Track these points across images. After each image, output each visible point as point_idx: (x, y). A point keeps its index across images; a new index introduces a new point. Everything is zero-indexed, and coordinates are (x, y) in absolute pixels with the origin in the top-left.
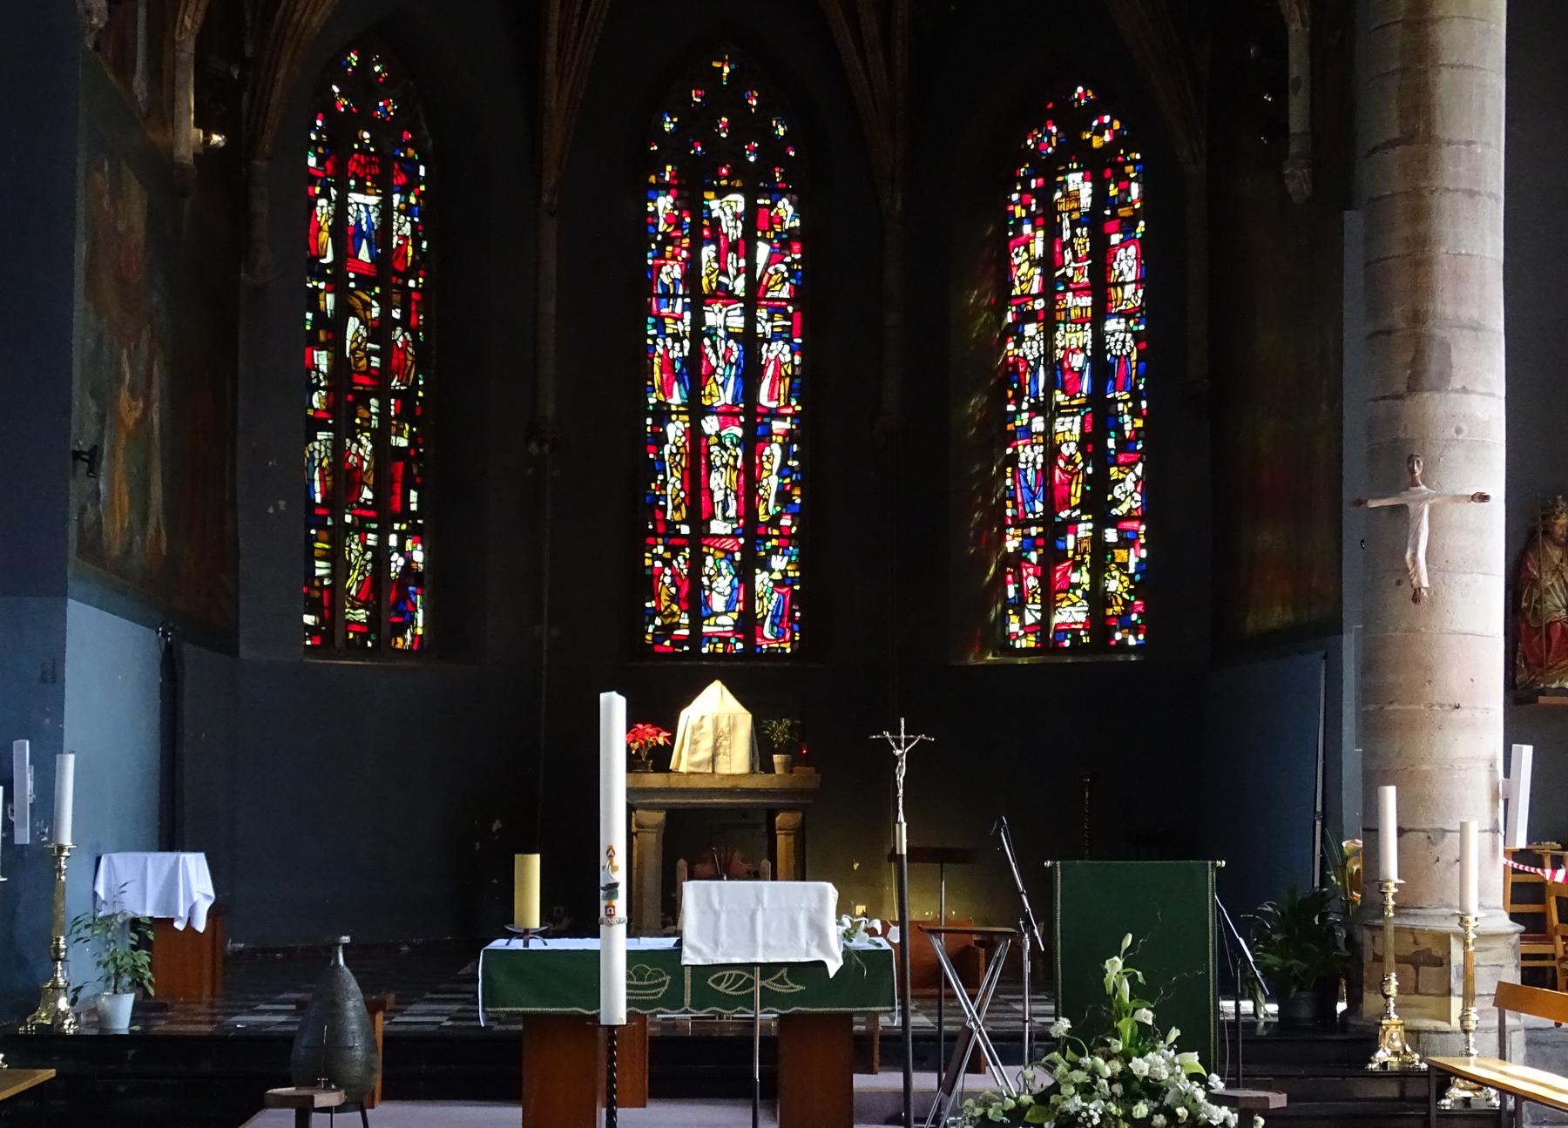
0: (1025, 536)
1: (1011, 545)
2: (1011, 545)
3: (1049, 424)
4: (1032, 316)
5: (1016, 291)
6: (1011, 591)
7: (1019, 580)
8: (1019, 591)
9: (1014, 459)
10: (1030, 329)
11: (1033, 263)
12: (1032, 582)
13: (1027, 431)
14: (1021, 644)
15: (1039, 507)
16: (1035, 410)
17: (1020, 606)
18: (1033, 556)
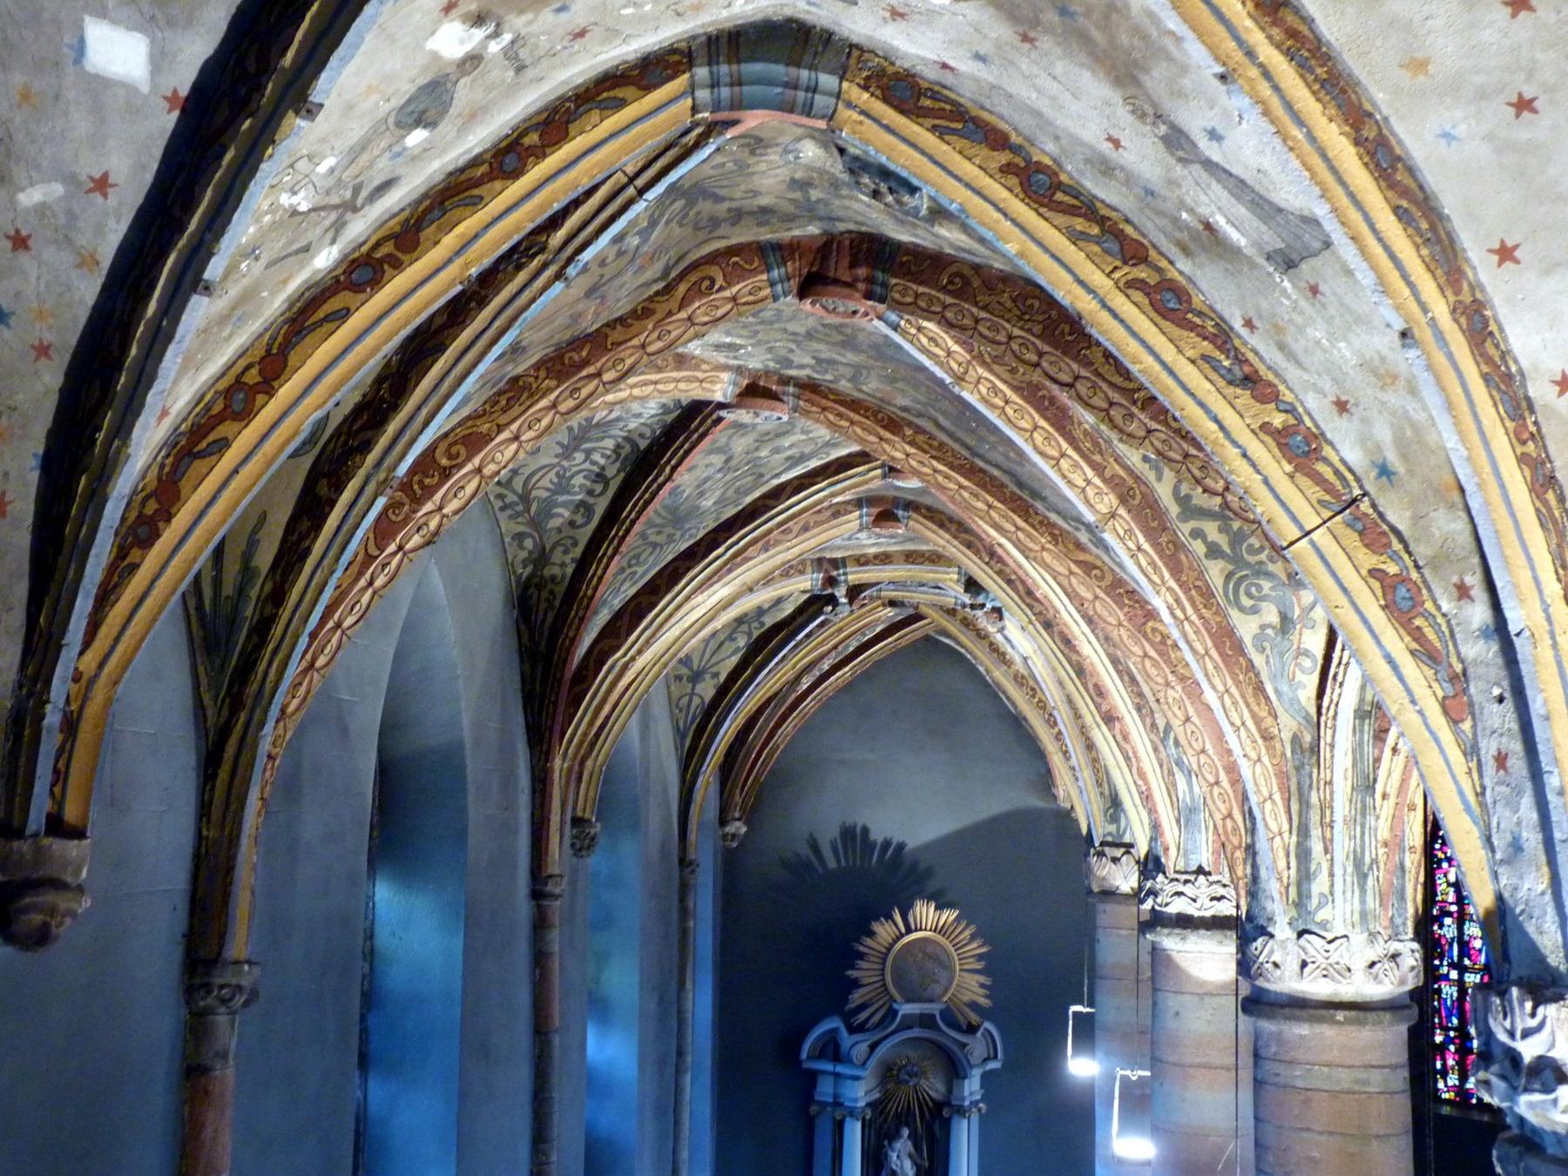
0: (1447, 1036)
1: (1439, 1039)
2: (1439, 1039)
3: (1461, 975)
4: (1450, 914)
5: (1439, 898)
6: (1439, 1065)
7: (1444, 1060)
8: (1444, 1065)
9: (1439, 991)
10: (1448, 921)
11: (1449, 885)
12: (1451, 1062)
13: (1446, 978)
14: (1445, 1096)
15: (1455, 1021)
16: (1452, 965)
17: (1444, 1073)
18: (1452, 1048)
